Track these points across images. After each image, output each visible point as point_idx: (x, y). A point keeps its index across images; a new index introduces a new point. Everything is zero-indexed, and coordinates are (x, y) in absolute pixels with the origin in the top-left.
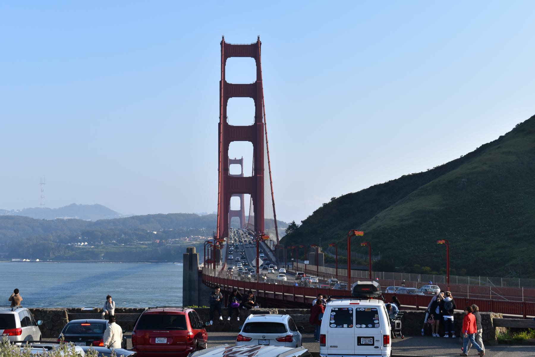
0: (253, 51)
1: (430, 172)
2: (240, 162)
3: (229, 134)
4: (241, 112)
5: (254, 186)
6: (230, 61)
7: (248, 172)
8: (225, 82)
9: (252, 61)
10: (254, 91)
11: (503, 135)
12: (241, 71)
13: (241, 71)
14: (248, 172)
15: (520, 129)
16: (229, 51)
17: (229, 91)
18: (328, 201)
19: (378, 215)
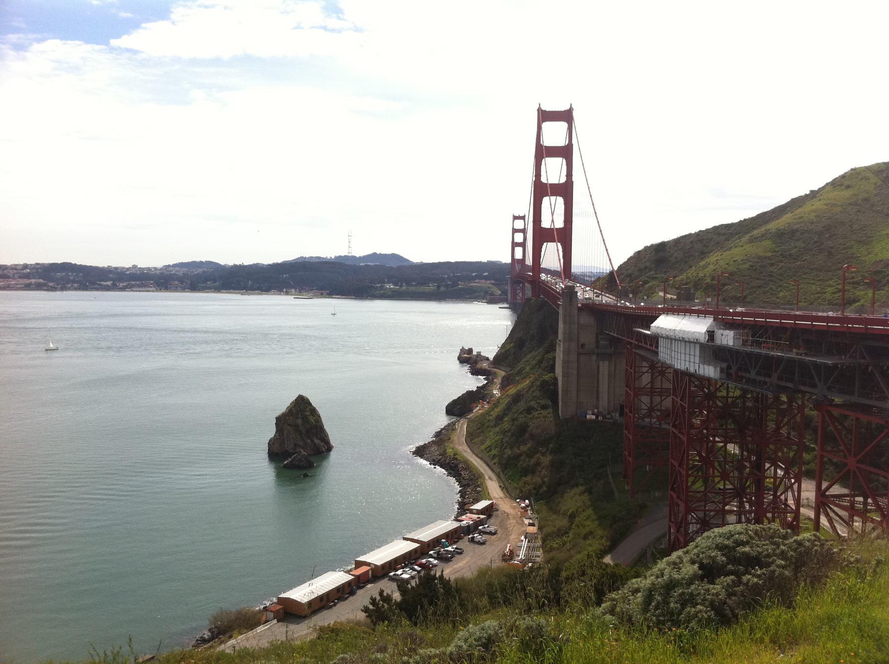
0: (566, 116)
1: (741, 223)
2: (523, 218)
3: (541, 190)
4: (554, 172)
5: (564, 236)
6: (546, 125)
7: (559, 224)
8: (541, 146)
9: (564, 125)
10: (565, 152)
11: (816, 189)
12: (554, 134)
13: (554, 134)
14: (559, 224)
15: (835, 184)
16: (545, 116)
17: (542, 152)
18: (640, 247)
19: (707, 260)
